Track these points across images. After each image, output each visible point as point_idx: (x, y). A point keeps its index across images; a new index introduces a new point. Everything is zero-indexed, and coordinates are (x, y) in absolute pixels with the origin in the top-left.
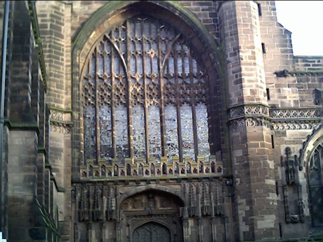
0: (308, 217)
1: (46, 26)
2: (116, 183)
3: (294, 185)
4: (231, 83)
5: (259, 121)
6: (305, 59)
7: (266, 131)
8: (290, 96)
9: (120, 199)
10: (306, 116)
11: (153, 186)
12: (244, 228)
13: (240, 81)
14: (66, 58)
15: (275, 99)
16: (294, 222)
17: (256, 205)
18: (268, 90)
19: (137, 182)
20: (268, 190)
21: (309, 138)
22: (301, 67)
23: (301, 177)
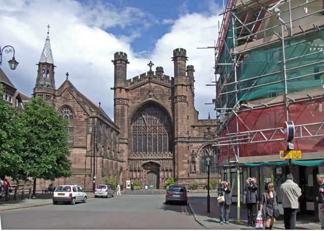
0: (198, 172)
1: (119, 113)
2: (140, 160)
3: (194, 162)
4: (175, 130)
5: (182, 142)
6: (201, 121)
7: (185, 145)
8: (195, 133)
9: (142, 164)
10: (201, 140)
11: (152, 161)
12: (176, 174)
13: (177, 130)
14: (126, 122)
15: (190, 135)
16: (193, 173)
17: (179, 168)
18: (188, 132)
19: (147, 160)
20: (185, 163)
21: (200, 147)
22: (200, 124)
23: (197, 160)
